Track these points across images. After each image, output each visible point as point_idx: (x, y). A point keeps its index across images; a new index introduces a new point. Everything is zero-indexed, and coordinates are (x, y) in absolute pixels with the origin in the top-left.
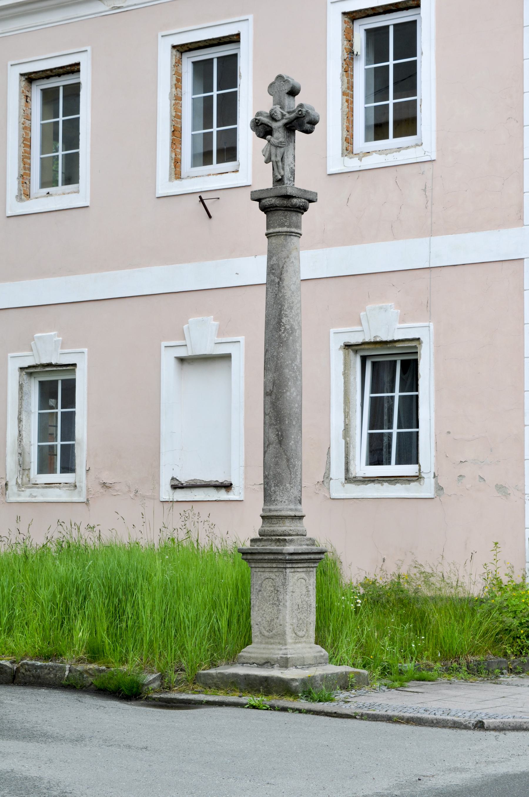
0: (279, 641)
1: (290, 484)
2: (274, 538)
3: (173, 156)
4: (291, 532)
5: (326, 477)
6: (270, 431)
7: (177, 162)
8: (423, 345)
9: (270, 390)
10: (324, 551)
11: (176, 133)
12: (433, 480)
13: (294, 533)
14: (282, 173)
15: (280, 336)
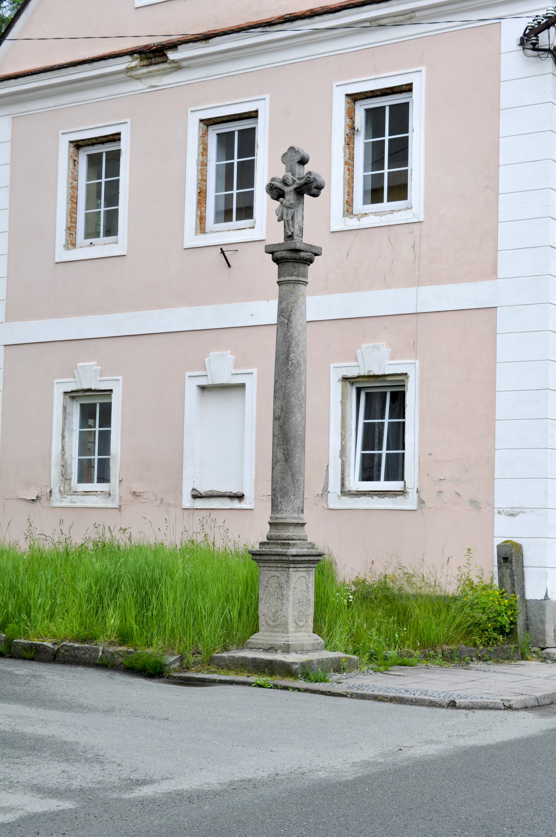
1: (294, 496)
2: (279, 542)
3: (199, 214)
4: (294, 537)
6: (278, 450)
7: (202, 219)
10: (322, 553)
11: (202, 193)
12: (416, 495)
13: (297, 538)
14: (292, 230)
15: (288, 369)
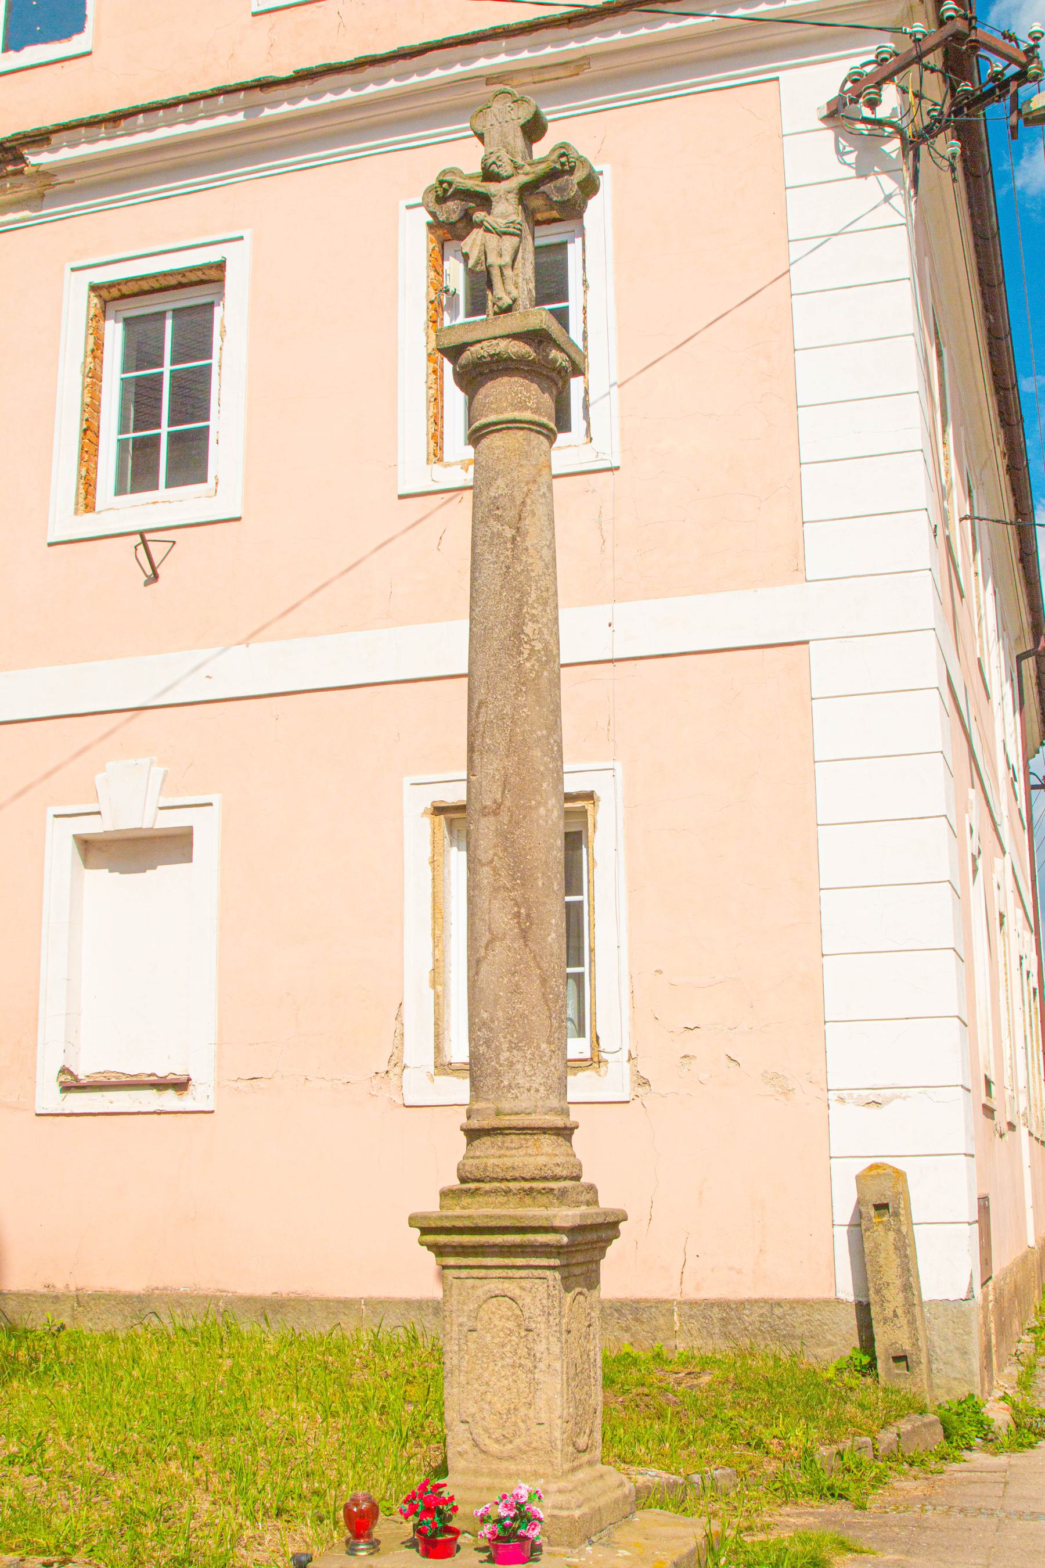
0: (534, 1467)
1: (549, 1043)
2: (513, 1185)
3: (84, 473)
4: (558, 1171)
5: (393, 1063)
6: (496, 904)
7: (88, 484)
8: (601, 805)
9: (495, 802)
10: (611, 1219)
11: (90, 432)
12: (627, 1066)
13: (565, 1173)
14: (515, 293)
15: (520, 666)
